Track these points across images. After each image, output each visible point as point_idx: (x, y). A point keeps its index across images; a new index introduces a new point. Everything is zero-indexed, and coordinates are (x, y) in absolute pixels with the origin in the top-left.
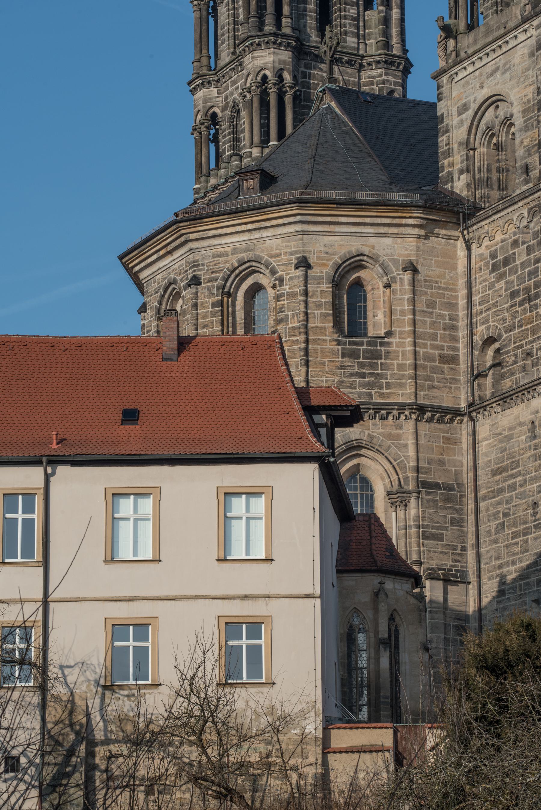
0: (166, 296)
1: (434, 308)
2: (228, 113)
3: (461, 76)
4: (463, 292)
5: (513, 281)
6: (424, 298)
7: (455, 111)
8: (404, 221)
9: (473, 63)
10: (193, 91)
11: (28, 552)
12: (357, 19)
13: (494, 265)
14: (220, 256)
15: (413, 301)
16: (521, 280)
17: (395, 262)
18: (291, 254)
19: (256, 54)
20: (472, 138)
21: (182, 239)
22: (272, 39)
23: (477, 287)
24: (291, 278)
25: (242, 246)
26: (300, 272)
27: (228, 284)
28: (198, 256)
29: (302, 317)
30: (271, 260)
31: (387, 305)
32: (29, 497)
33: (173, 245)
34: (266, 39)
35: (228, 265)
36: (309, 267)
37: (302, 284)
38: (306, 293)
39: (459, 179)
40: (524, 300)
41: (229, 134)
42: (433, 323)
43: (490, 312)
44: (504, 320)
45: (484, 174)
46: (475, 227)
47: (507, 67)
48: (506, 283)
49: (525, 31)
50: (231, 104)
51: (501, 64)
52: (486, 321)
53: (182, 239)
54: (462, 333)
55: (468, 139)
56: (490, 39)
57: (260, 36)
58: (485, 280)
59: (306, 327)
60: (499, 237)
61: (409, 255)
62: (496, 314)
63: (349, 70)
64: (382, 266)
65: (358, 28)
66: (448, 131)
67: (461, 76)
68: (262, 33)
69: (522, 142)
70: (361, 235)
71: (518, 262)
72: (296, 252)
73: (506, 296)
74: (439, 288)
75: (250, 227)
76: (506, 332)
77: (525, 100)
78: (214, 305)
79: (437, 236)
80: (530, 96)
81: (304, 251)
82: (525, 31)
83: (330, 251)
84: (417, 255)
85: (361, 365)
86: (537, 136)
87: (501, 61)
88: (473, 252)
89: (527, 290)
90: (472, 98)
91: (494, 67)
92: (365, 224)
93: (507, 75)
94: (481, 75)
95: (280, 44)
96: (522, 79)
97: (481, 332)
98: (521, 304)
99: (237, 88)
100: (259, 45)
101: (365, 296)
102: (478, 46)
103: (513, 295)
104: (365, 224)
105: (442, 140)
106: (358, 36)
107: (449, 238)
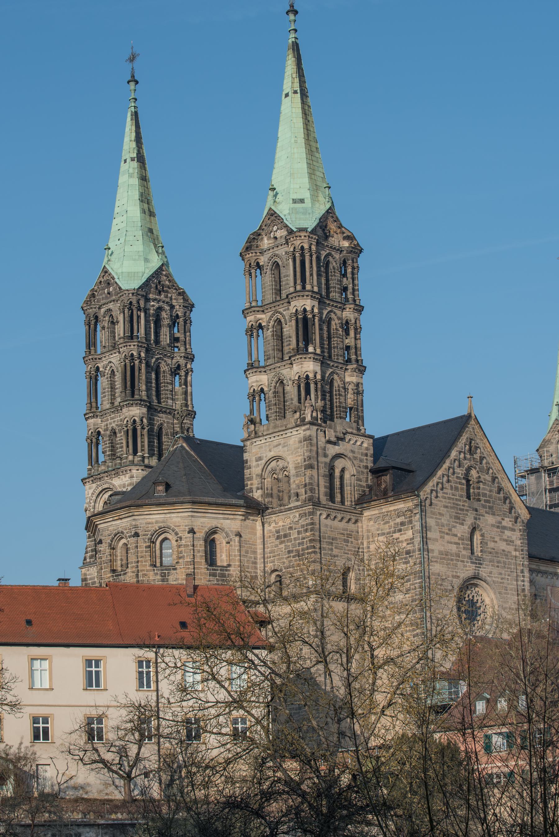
0: (115, 538)
1: (248, 553)
2: (108, 433)
3: (257, 443)
4: (260, 547)
6: (244, 549)
7: (254, 459)
8: (237, 513)
9: (266, 439)
10: (87, 419)
11: (149, 686)
12: (172, 391)
13: (278, 536)
14: (149, 524)
15: (240, 551)
16: (294, 546)
17: (232, 531)
18: (186, 526)
19: (131, 408)
20: (263, 473)
21: (131, 514)
22: (139, 402)
23: (268, 545)
24: (186, 538)
25: (161, 520)
26: (191, 535)
27: (153, 537)
28: (138, 523)
29: (192, 557)
30: (176, 528)
31: (228, 552)
32: (148, 662)
33: (124, 516)
34: (136, 402)
35: (153, 529)
36: (194, 533)
37: (192, 541)
38: (193, 546)
39: (256, 492)
40: (296, 555)
41: (109, 443)
42: (248, 561)
43: (276, 558)
44: (284, 563)
45: (270, 491)
46: (267, 517)
47: (286, 444)
48: (285, 546)
49: (297, 431)
50: (110, 428)
51: (282, 442)
52: (274, 562)
53: (131, 514)
54: (260, 566)
55: (262, 474)
56: (277, 430)
57: (133, 400)
58: (272, 543)
59: (194, 561)
60: (281, 524)
61: (238, 528)
62: (279, 559)
63: (169, 417)
64: (226, 533)
65: (172, 395)
66: (250, 468)
67: (257, 443)
68: (133, 399)
69: (294, 481)
70: (217, 518)
71: (292, 537)
72: (188, 525)
73: (285, 552)
74: (250, 544)
75: (166, 511)
76: (285, 568)
77: (297, 462)
78: (146, 547)
79: (249, 519)
80: (299, 461)
81: (192, 525)
82: (297, 431)
83: (204, 525)
84: (241, 529)
85: (218, 580)
86: (304, 480)
88: (265, 528)
89: (298, 551)
91: (277, 443)
92: (219, 514)
93: (286, 448)
94: (270, 445)
95: (142, 405)
96: (294, 452)
97: (270, 566)
98: (294, 557)
99: (114, 422)
100: (132, 404)
101: (216, 546)
102: (270, 432)
103: (289, 552)
104: (219, 514)
105: (246, 472)
106: (173, 399)
107: (253, 520)
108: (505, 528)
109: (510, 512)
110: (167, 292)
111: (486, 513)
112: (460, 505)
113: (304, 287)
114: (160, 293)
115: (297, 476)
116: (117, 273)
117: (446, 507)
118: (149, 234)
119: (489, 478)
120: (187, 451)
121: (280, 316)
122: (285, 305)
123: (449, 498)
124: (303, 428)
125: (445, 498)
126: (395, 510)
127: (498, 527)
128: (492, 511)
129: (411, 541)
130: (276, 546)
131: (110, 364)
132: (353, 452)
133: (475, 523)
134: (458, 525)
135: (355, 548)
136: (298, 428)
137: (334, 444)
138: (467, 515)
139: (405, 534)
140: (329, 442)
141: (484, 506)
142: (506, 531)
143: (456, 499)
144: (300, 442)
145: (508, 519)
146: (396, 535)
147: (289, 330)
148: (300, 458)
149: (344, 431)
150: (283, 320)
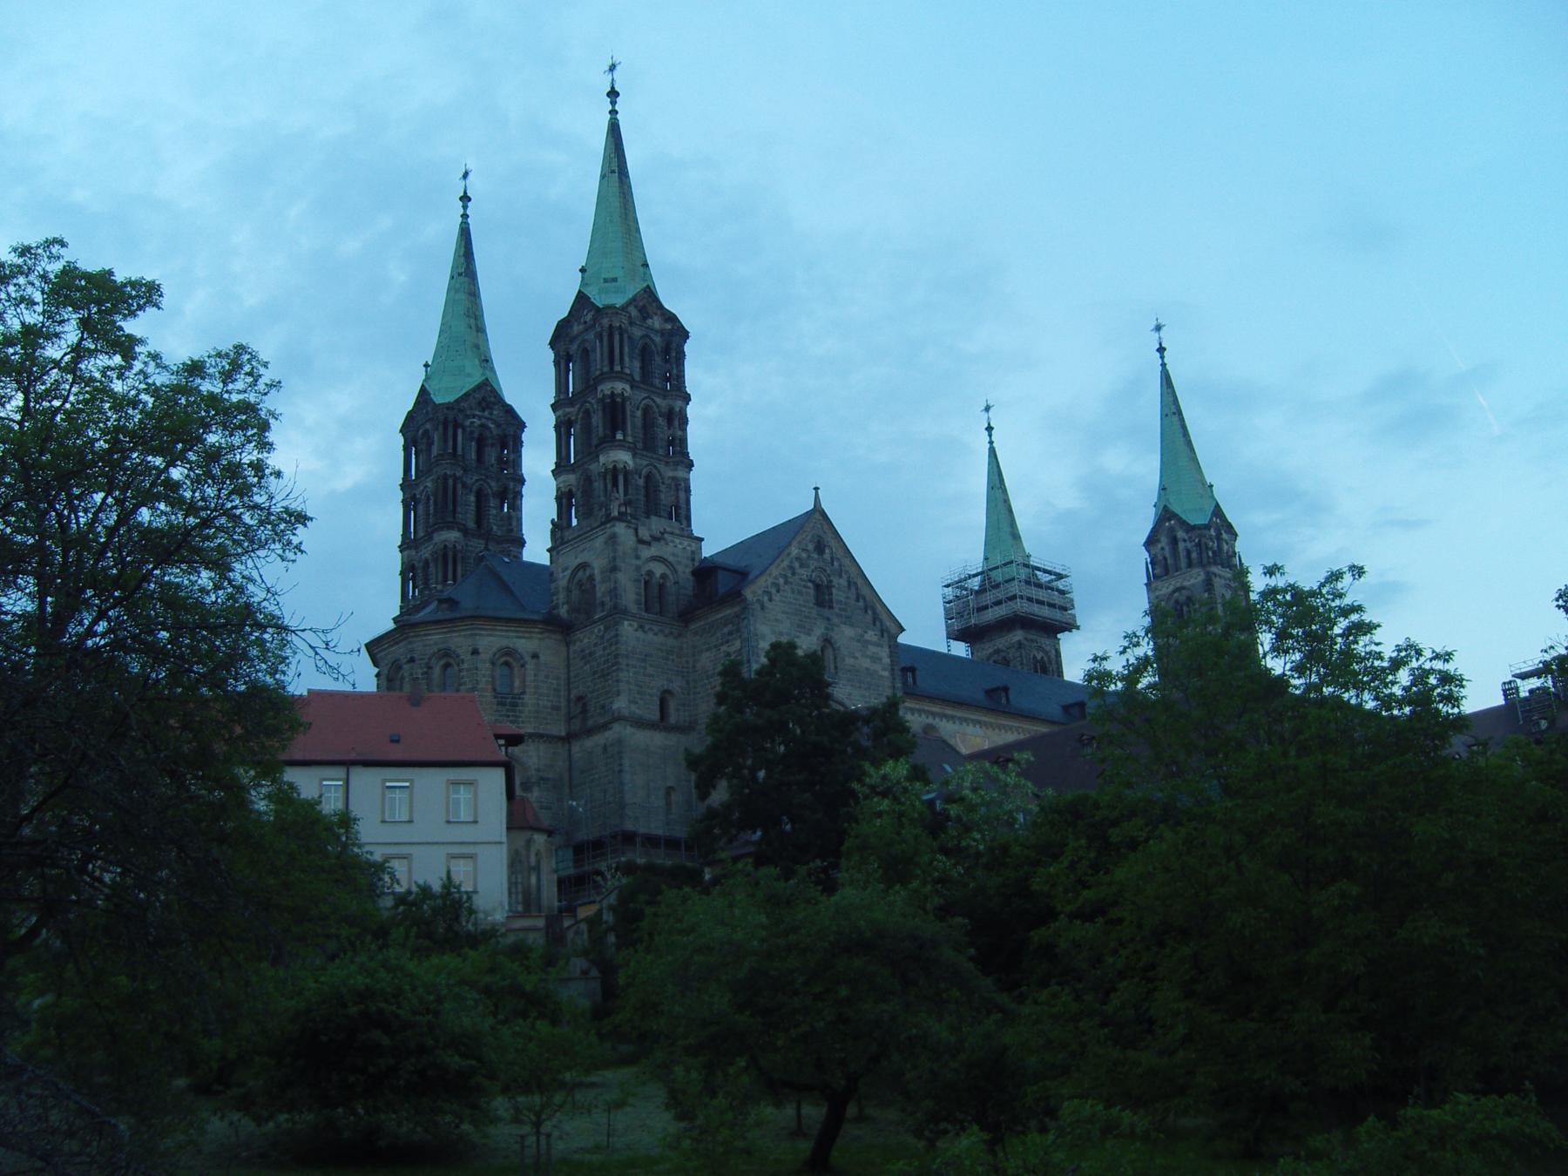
7: (560, 570)
14: (426, 645)
98: (599, 678)
108: (868, 642)
109: (874, 625)
110: (492, 409)
111: (841, 623)
112: (804, 612)
113: (612, 368)
114: (483, 410)
117: (786, 613)
118: (474, 349)
119: (843, 582)
123: (790, 603)
125: (784, 602)
127: (858, 641)
128: (848, 620)
130: (582, 667)
132: (674, 555)
133: (827, 634)
134: (802, 635)
135: (678, 667)
137: (648, 544)
138: (815, 624)
139: (733, 645)
140: (641, 541)
141: (839, 616)
142: (870, 647)
143: (800, 605)
144: (606, 543)
145: (873, 633)
146: (724, 648)
147: (597, 419)
149: (662, 531)
150: (591, 410)
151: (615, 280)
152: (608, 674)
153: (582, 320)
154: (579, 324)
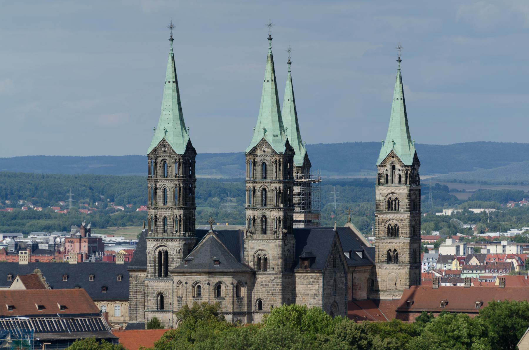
5: (268, 290)
7: (250, 248)
19: (180, 211)
44: (265, 296)
52: (259, 295)
60: (264, 279)
69: (272, 262)
78: (213, 289)
80: (275, 254)
87: (266, 244)
89: (273, 293)
90: (256, 247)
93: (268, 247)
98: (270, 295)
115: (273, 260)
116: (171, 143)
120: (215, 239)
121: (265, 187)
122: (269, 183)
124: (278, 241)
126: (310, 276)
129: (317, 290)
131: (164, 185)
136: (275, 240)
146: (310, 286)
148: (276, 253)
150: (267, 189)
151: (277, 136)
152: (275, 295)
153: (263, 149)
154: (261, 150)
